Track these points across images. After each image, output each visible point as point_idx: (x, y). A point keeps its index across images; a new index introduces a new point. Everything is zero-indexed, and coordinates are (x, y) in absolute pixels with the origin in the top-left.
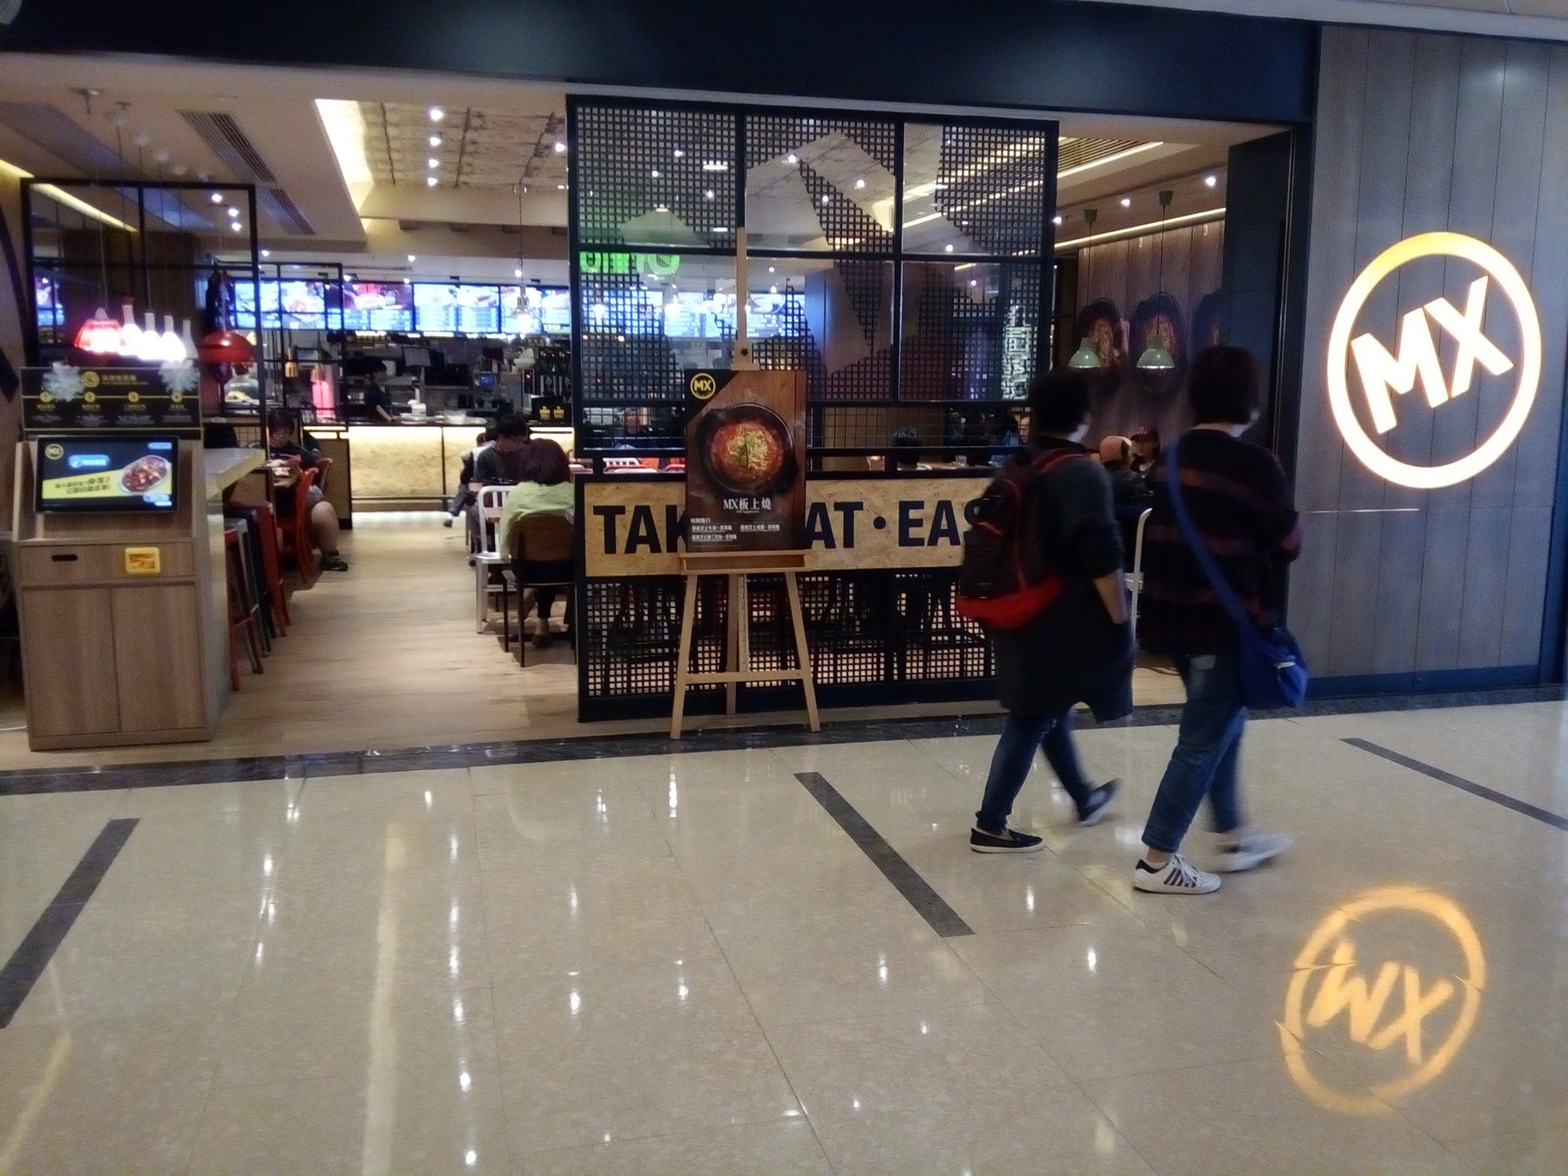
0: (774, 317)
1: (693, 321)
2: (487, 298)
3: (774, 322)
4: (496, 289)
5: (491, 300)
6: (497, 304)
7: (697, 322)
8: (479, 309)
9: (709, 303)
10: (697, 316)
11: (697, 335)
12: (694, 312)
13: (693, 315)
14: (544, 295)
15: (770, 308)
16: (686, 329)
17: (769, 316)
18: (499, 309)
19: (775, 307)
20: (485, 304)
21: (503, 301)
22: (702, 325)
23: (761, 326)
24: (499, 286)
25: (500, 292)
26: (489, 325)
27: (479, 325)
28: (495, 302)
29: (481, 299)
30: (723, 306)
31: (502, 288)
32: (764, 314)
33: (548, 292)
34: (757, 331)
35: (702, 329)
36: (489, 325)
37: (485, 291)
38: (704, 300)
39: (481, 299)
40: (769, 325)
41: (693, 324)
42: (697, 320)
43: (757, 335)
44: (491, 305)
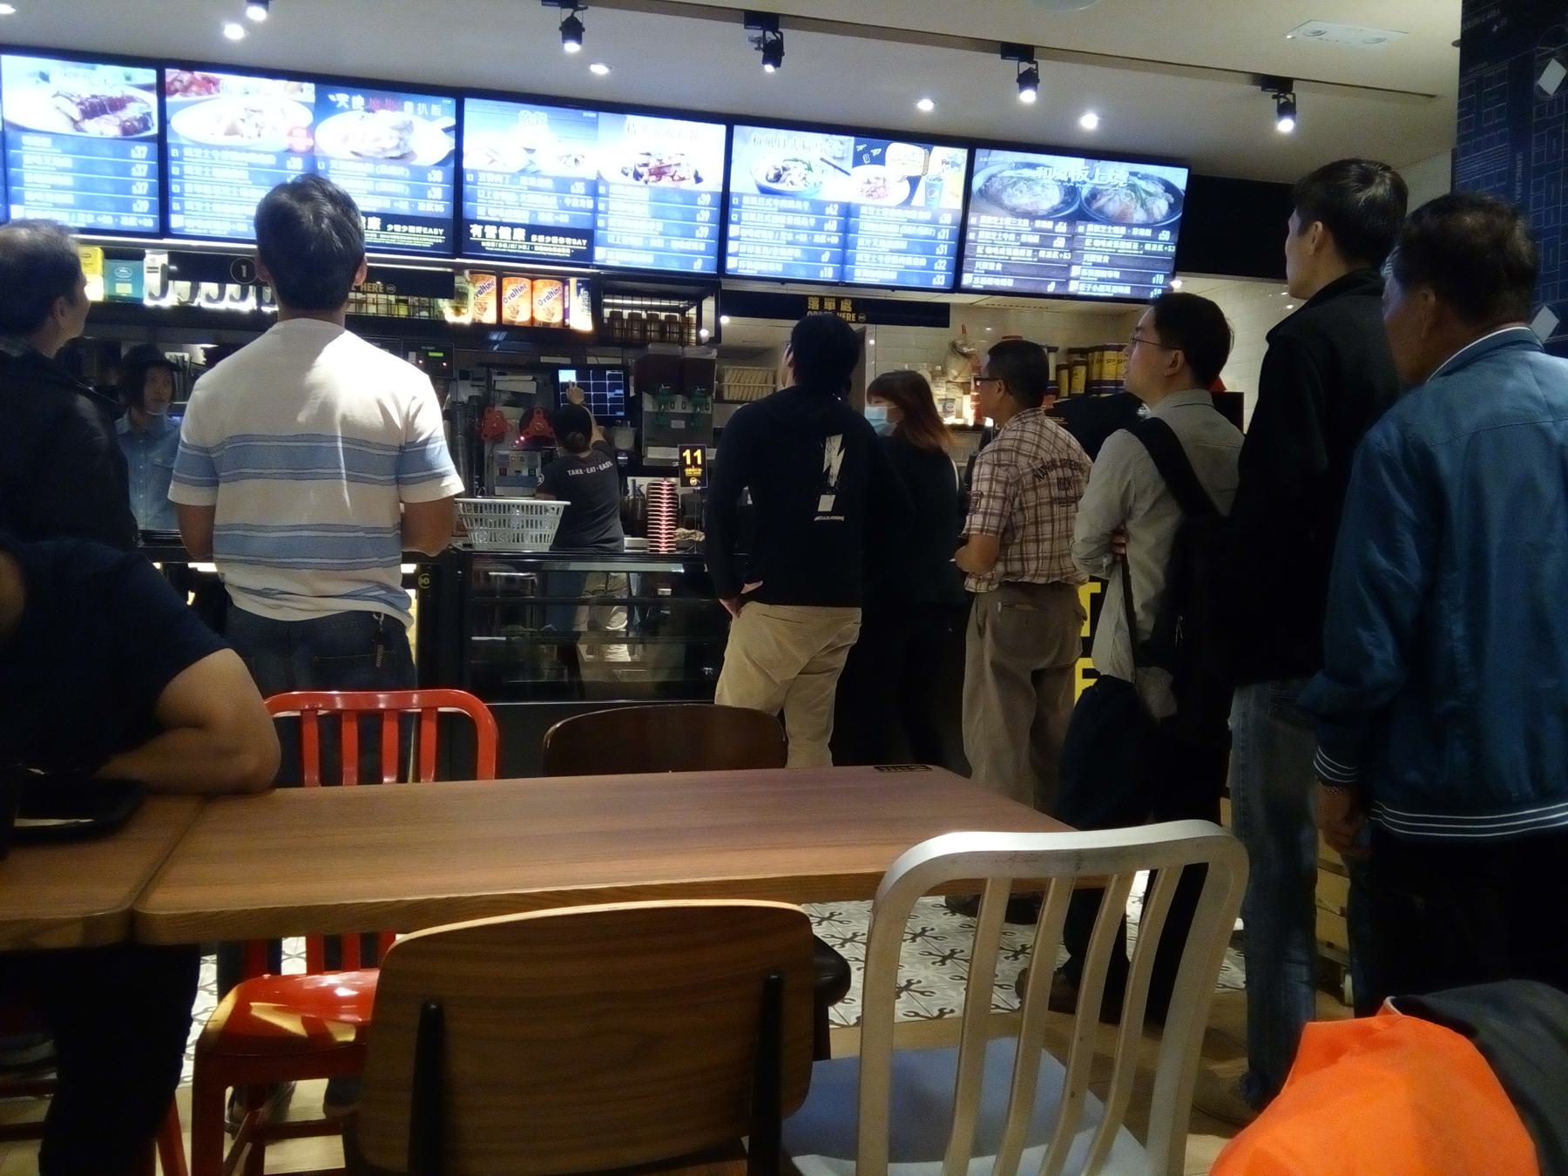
0: (1062, 227)
1: (819, 227)
2: (116, 105)
3: (1060, 242)
4: (149, 76)
5: (132, 112)
6: (154, 131)
7: (830, 235)
8: (85, 146)
9: (868, 171)
10: (832, 211)
11: (828, 274)
12: (824, 196)
13: (818, 208)
14: (323, 108)
15: (1053, 198)
16: (797, 253)
17: (1048, 225)
18: (161, 144)
19: (1071, 192)
20: (107, 127)
21: (177, 122)
22: (845, 245)
23: (1026, 255)
24: (159, 64)
25: (162, 89)
26: (126, 207)
27: (86, 205)
28: (144, 121)
29: (94, 109)
30: (914, 182)
31: (171, 74)
32: (1032, 216)
33: (340, 98)
34: (1008, 269)
35: (843, 258)
36: (126, 207)
37: (108, 80)
38: (858, 161)
39: (94, 109)
40: (1042, 254)
41: (820, 238)
42: (832, 226)
43: (1007, 283)
44: (130, 132)
